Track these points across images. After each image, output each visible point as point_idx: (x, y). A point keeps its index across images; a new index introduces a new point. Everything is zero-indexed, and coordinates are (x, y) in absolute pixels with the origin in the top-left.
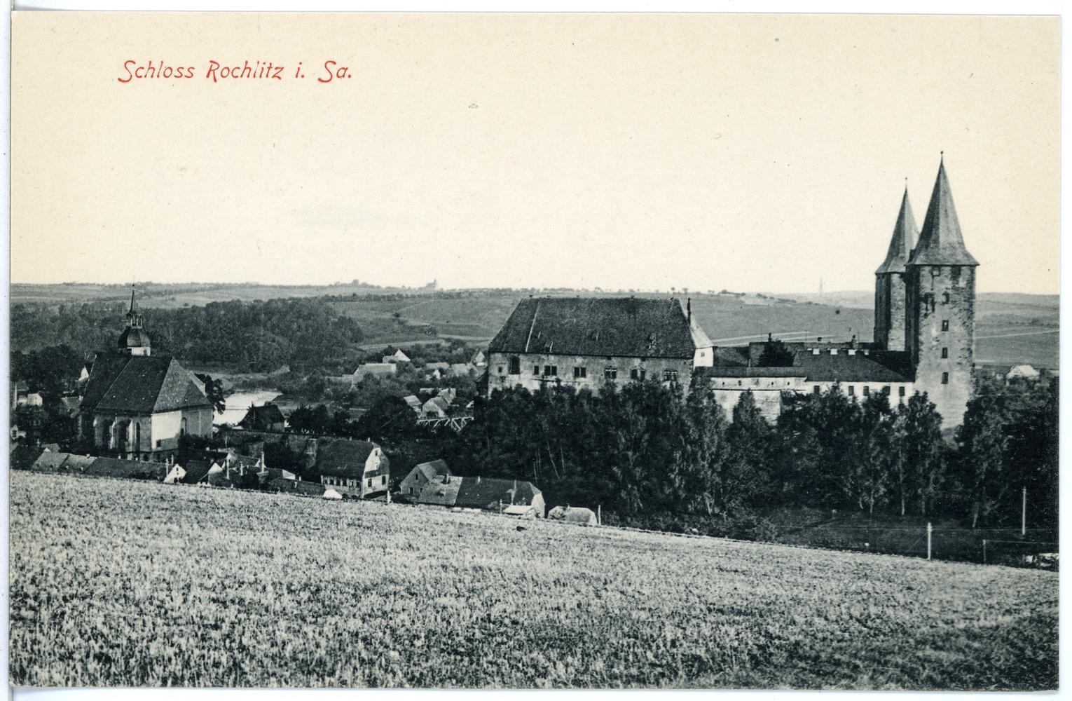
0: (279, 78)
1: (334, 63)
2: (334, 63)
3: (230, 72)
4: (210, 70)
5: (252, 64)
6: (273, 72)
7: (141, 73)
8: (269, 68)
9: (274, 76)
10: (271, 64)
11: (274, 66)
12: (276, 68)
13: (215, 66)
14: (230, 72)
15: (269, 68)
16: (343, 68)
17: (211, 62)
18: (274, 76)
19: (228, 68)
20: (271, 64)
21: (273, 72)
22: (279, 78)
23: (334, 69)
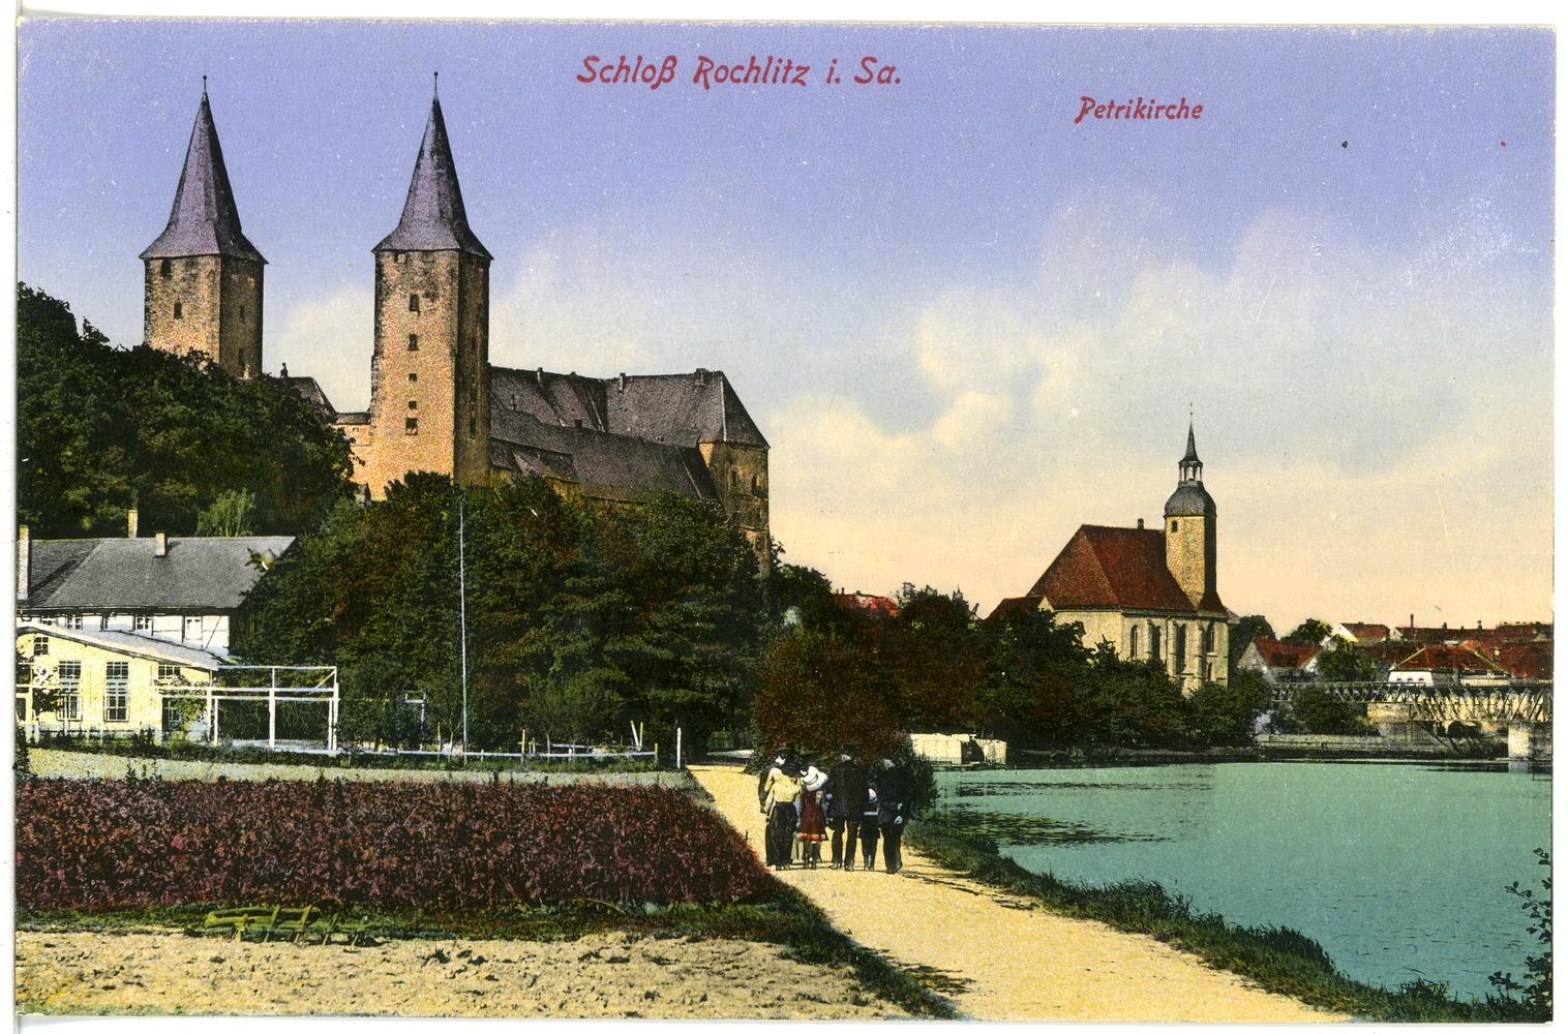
0: (803, 83)
1: (874, 60)
2: (874, 60)
3: (727, 74)
4: (700, 71)
5: (762, 63)
6: (793, 73)
7: (609, 74)
8: (788, 68)
9: (795, 80)
10: (790, 62)
11: (795, 65)
12: (799, 68)
13: (707, 66)
14: (727, 74)
15: (788, 68)
16: (887, 68)
17: (701, 58)
18: (795, 80)
19: (726, 68)
20: (790, 62)
21: (793, 73)
22: (803, 83)
23: (874, 68)
